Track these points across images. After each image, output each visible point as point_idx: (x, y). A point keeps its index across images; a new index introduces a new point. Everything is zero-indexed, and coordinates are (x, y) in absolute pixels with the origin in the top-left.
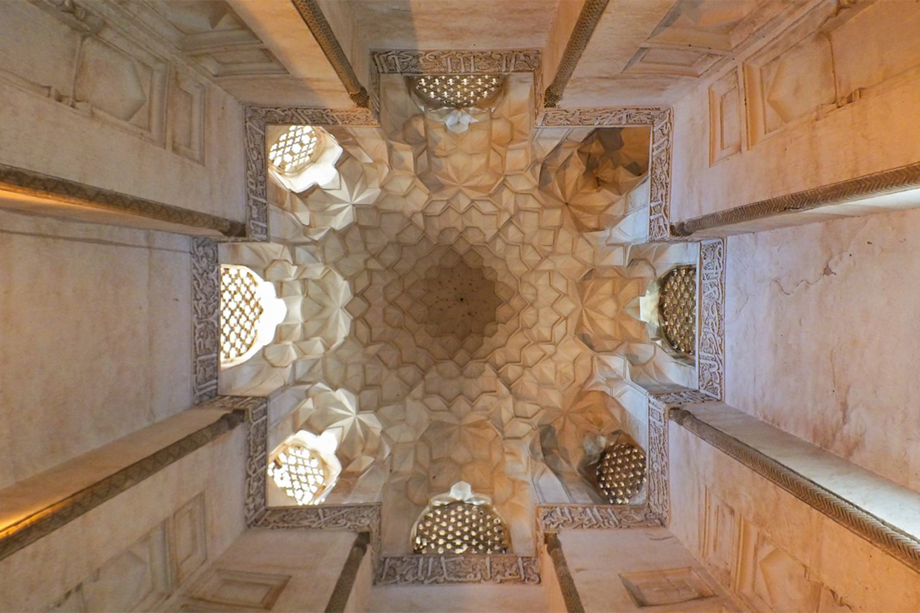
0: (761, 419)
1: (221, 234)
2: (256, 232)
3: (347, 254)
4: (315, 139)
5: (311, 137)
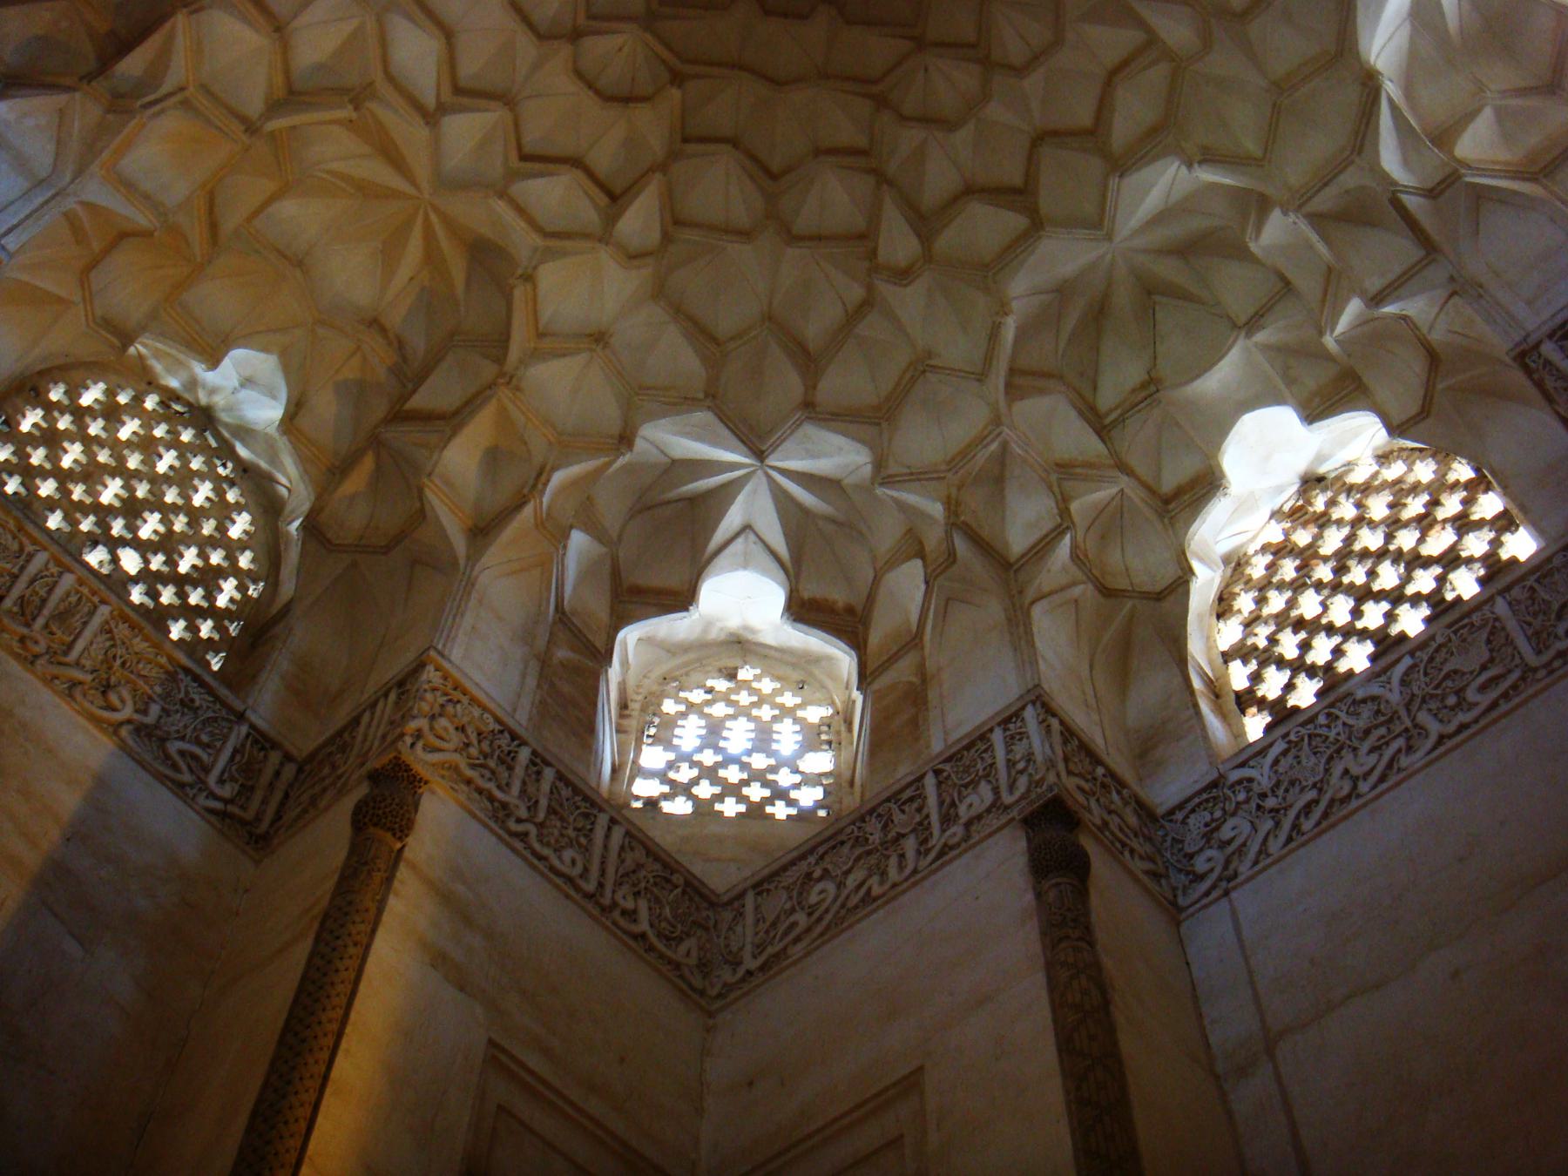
2: (1029, 757)
3: (923, 366)
4: (669, 706)
5: (670, 723)
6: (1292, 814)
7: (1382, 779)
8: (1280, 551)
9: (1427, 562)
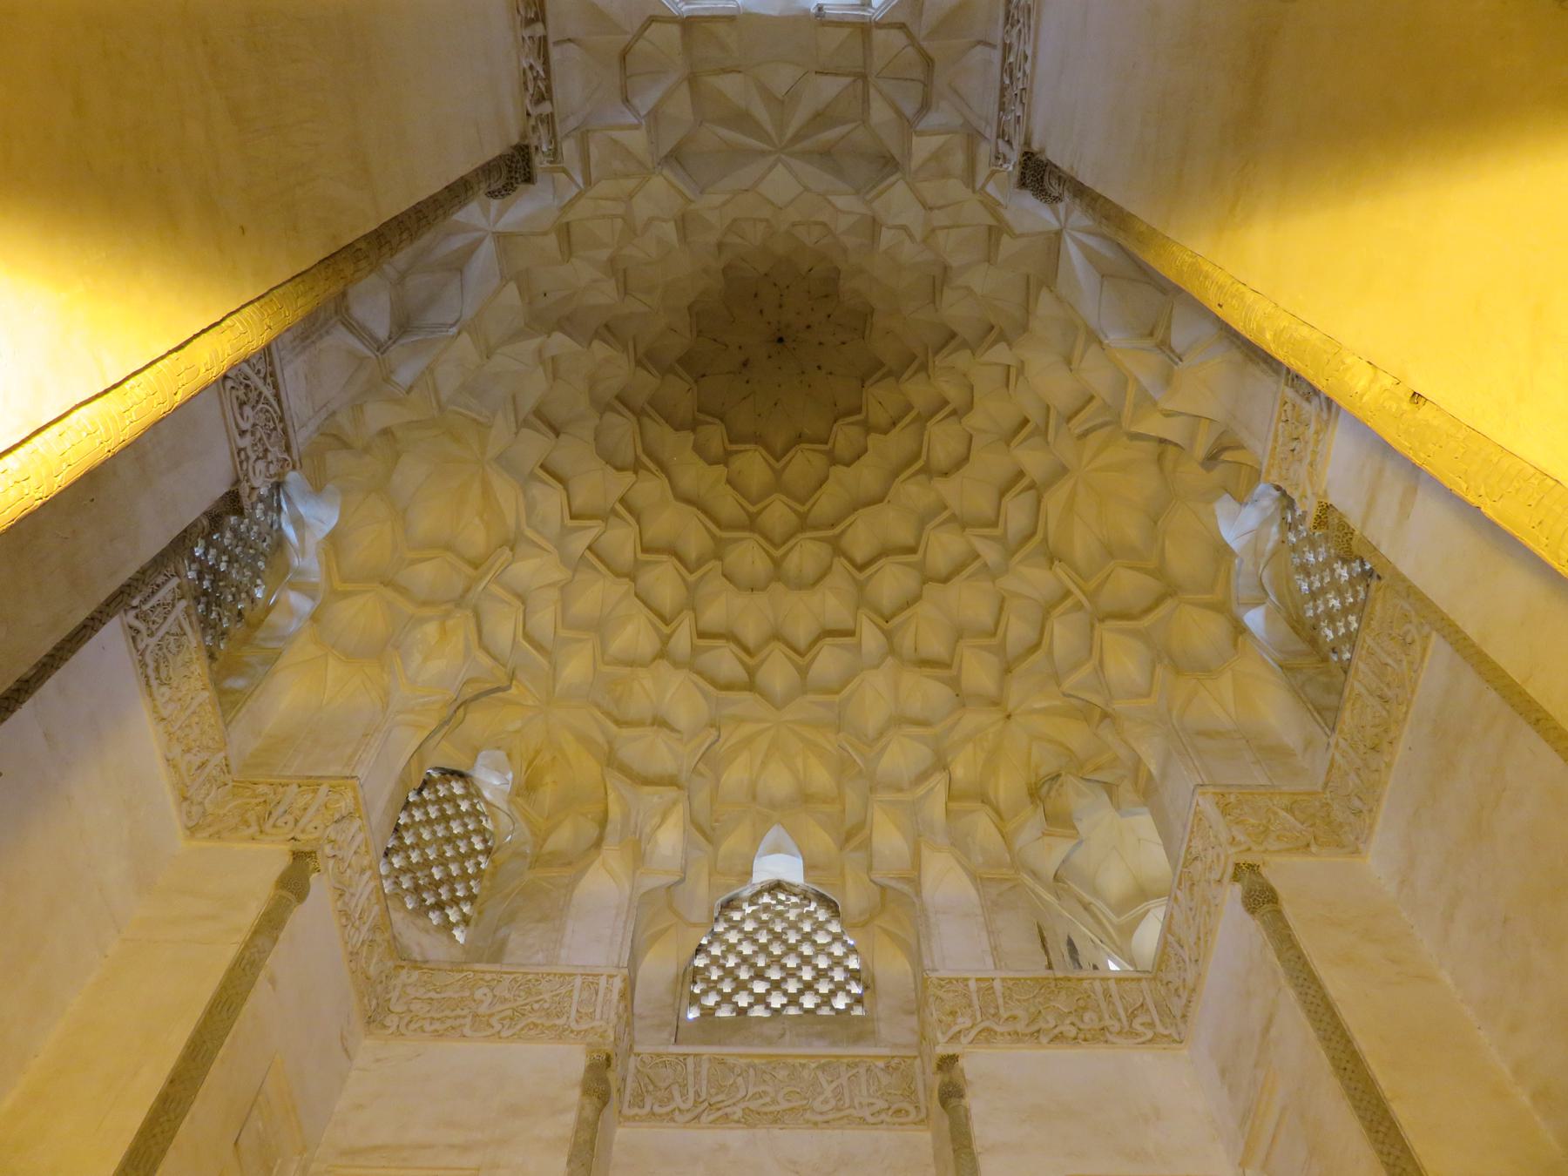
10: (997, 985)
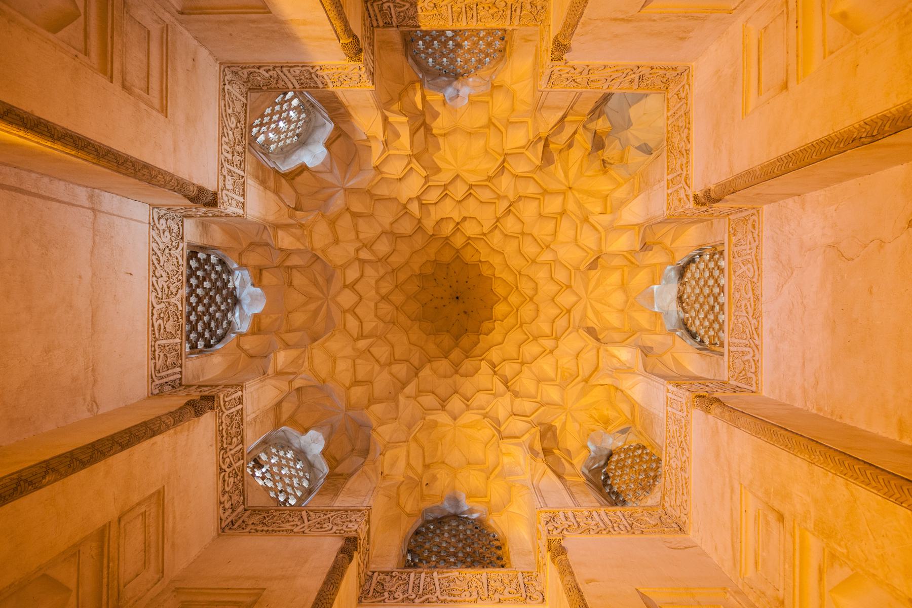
0: (814, 411)
1: (188, 202)
4: (303, 116)
5: (300, 113)
6: (160, 255)
7: (153, 285)
8: (225, 284)
9: (197, 321)
10: (670, 177)
